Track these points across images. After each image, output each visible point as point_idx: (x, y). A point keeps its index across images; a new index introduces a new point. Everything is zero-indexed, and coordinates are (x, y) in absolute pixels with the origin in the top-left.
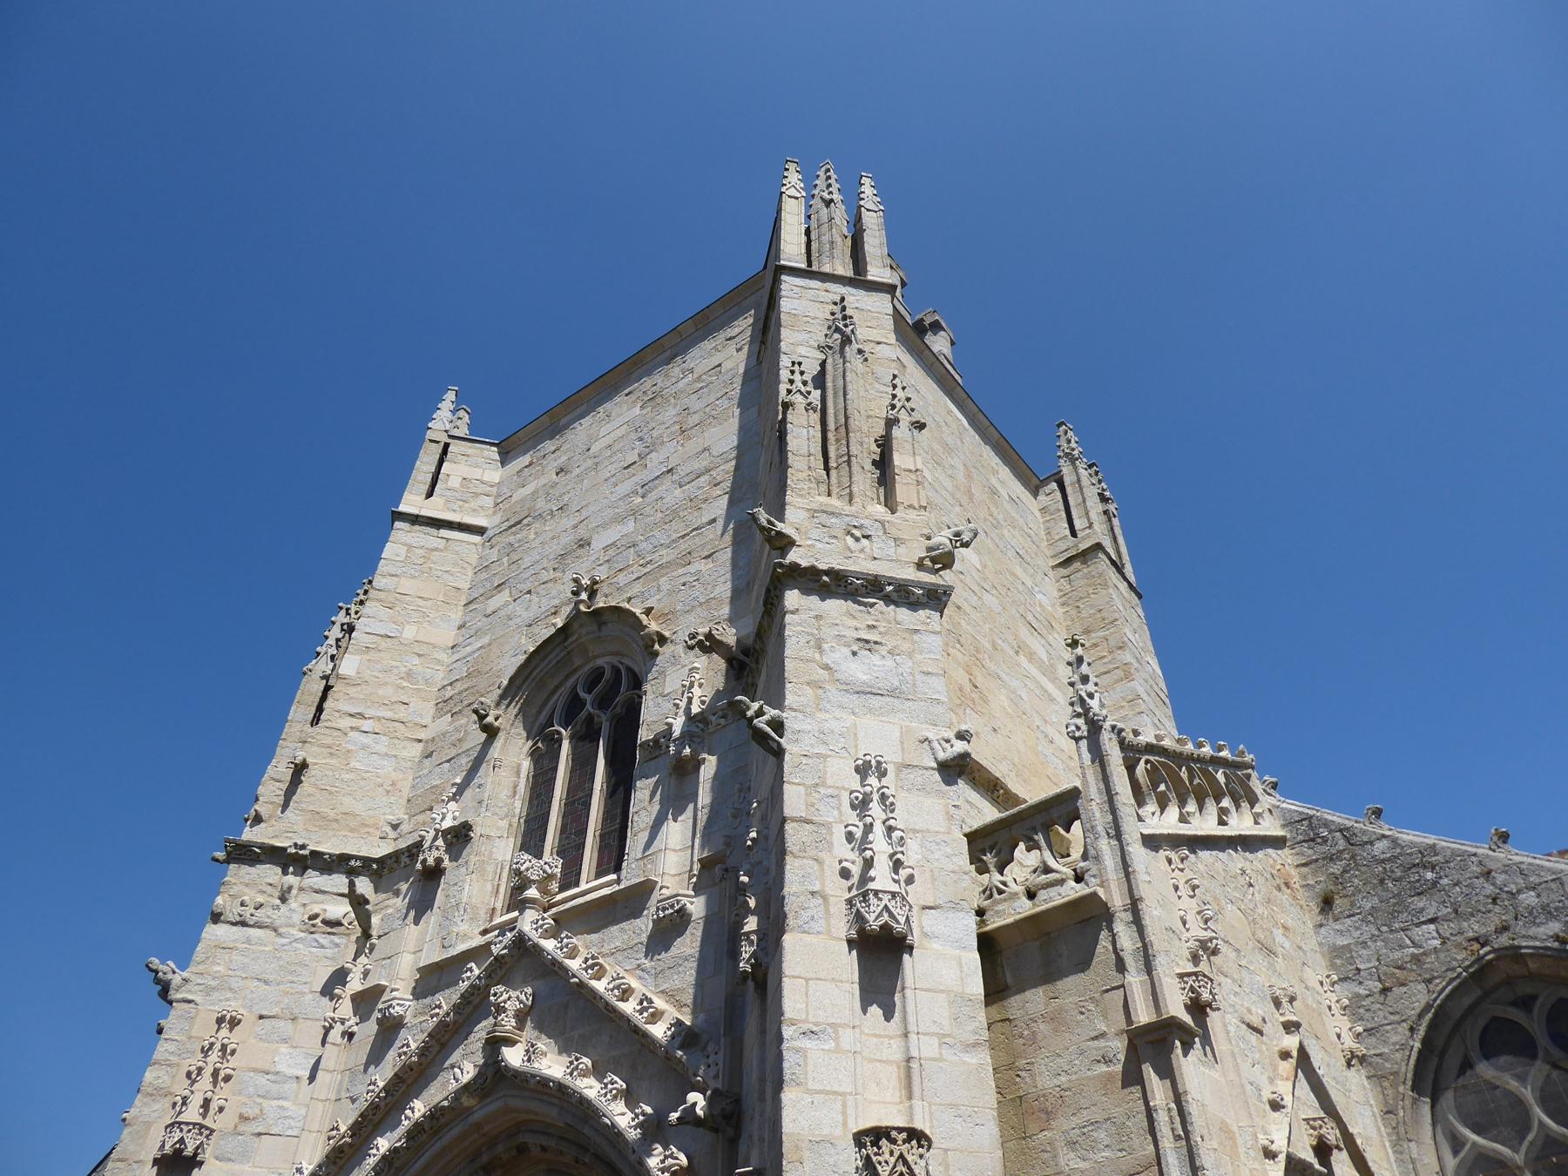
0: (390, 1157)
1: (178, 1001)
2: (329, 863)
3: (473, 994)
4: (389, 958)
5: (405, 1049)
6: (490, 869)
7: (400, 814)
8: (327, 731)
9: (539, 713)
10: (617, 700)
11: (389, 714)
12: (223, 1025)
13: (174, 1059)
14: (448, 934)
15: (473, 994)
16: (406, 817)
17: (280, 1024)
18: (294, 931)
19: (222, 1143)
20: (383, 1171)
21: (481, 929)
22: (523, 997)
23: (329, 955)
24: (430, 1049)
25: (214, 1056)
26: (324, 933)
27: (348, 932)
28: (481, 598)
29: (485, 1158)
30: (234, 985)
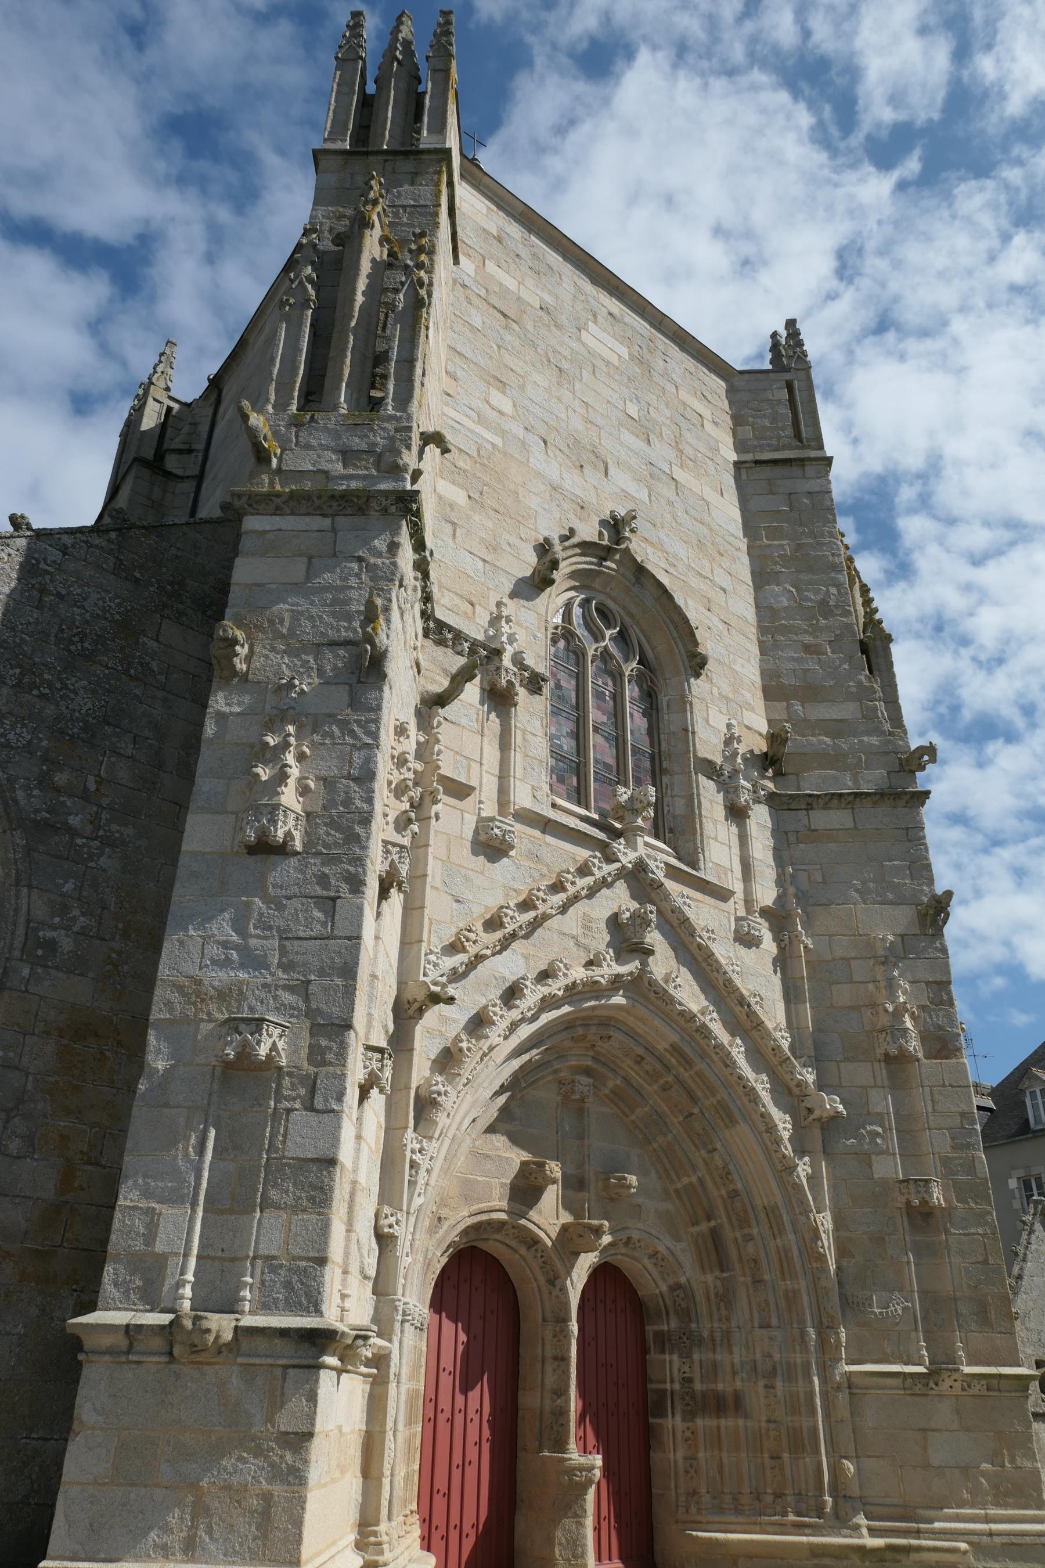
28: (472, 366)
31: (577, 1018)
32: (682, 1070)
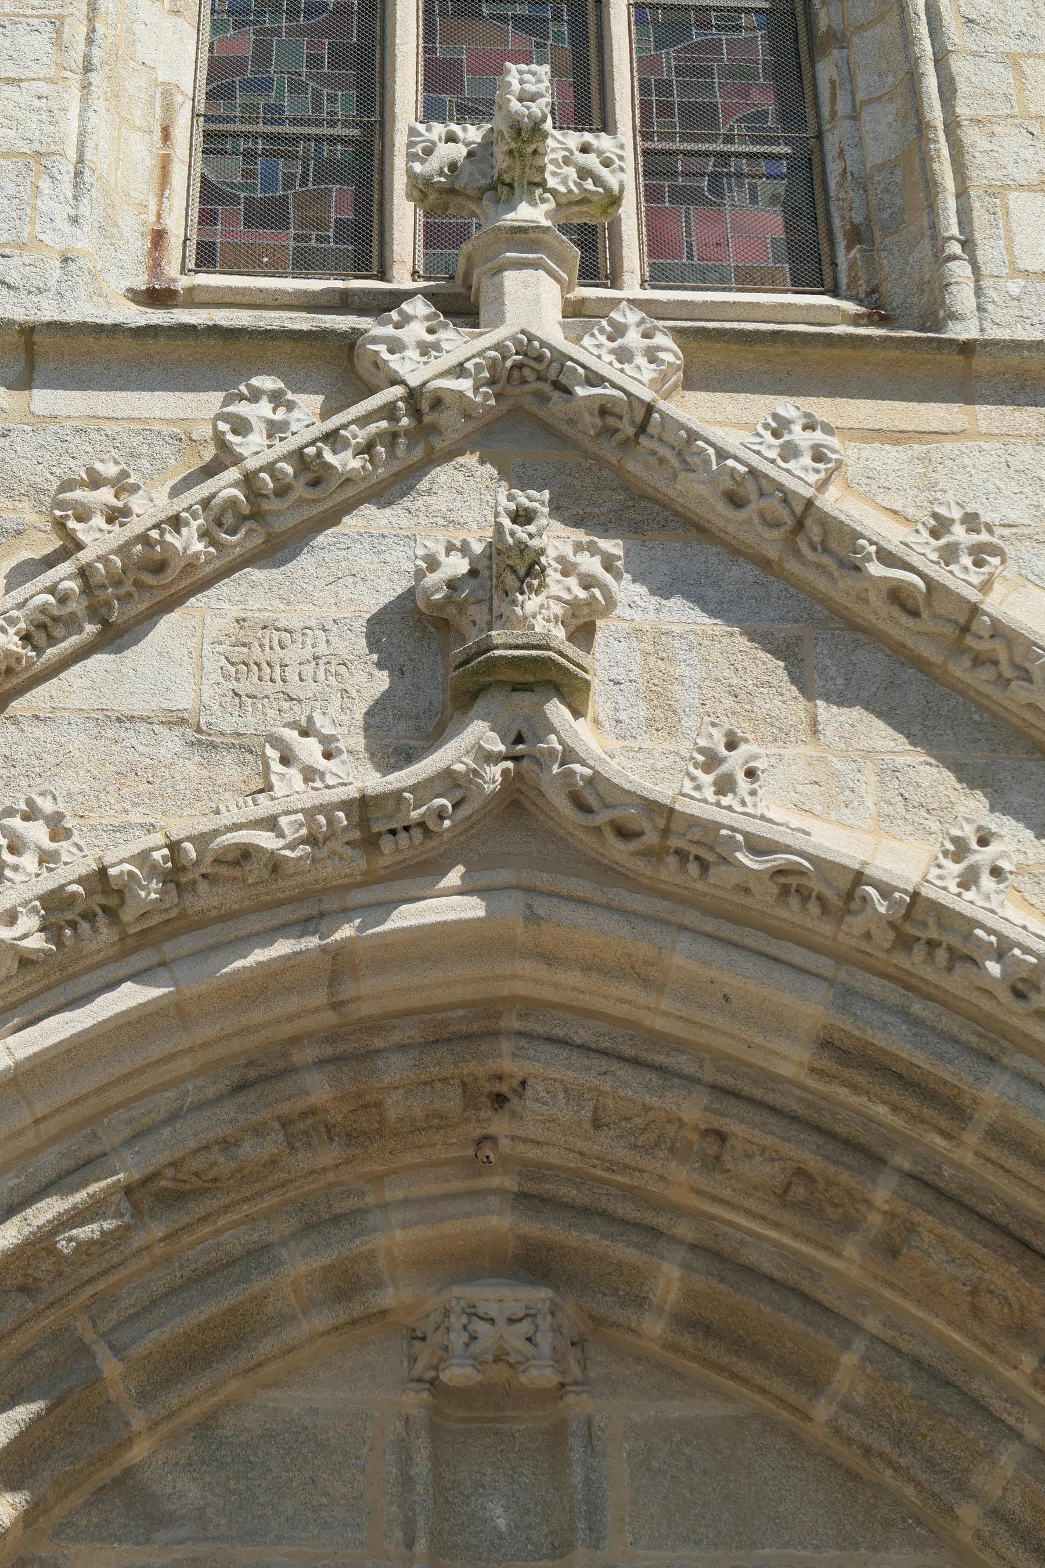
24: (58, 631)
31: (295, 1040)
32: (938, 1140)
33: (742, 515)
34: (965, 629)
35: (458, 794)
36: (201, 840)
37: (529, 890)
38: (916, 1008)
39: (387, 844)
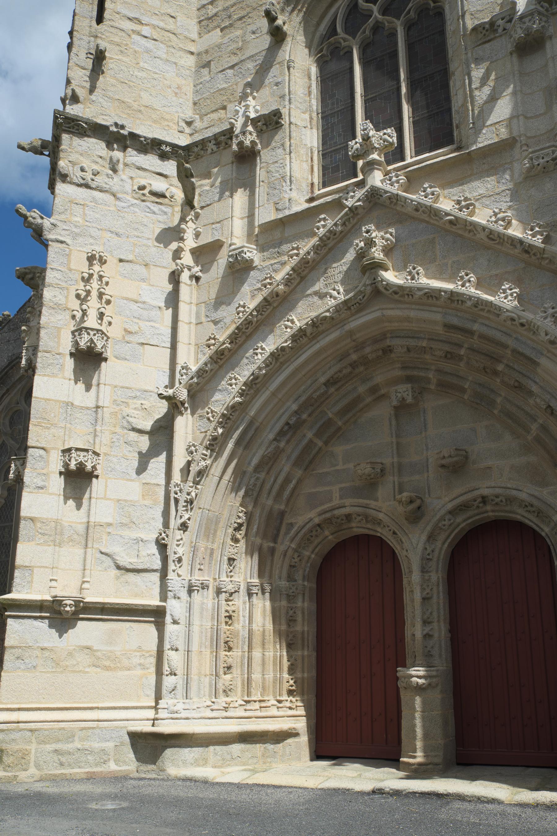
0: (276, 355)
1: (52, 241)
2: (145, 145)
3: (329, 239)
4: (218, 222)
5: (268, 281)
6: (302, 151)
7: (189, 114)
8: (112, 30)
9: (318, 24)
10: (410, 5)
11: (162, 24)
12: (95, 262)
13: (64, 285)
14: (281, 199)
15: (329, 239)
16: (197, 116)
17: (137, 267)
18: (129, 198)
19: (117, 347)
20: (271, 364)
21: (308, 197)
22: (388, 236)
23: (161, 220)
24: (293, 281)
25: (95, 285)
26: (153, 202)
27: (171, 203)
29: (354, 357)
30: (93, 234)
33: (419, 213)
34: (466, 225)
35: (363, 294)
36: (317, 317)
37: (383, 309)
38: (459, 314)
39: (352, 308)
